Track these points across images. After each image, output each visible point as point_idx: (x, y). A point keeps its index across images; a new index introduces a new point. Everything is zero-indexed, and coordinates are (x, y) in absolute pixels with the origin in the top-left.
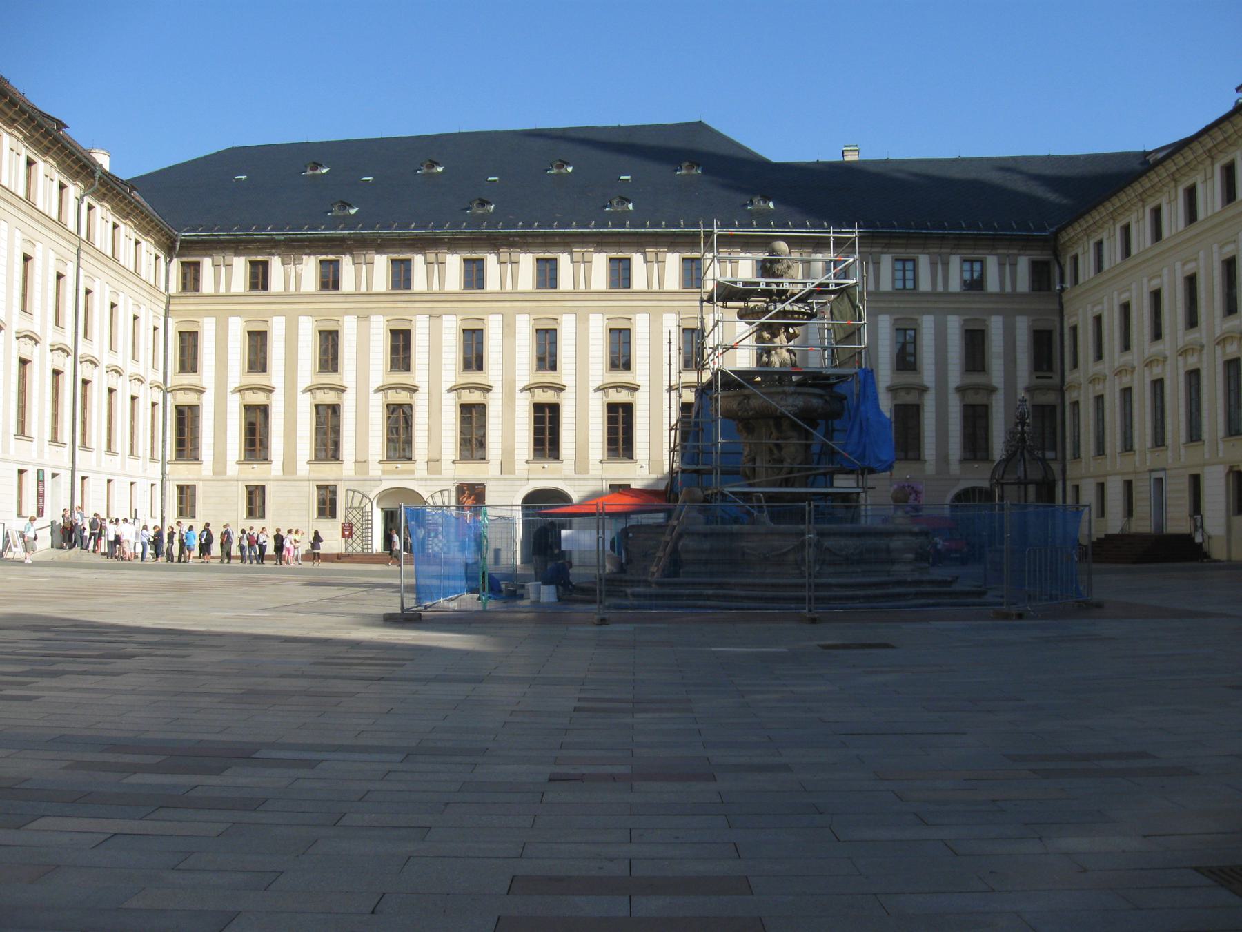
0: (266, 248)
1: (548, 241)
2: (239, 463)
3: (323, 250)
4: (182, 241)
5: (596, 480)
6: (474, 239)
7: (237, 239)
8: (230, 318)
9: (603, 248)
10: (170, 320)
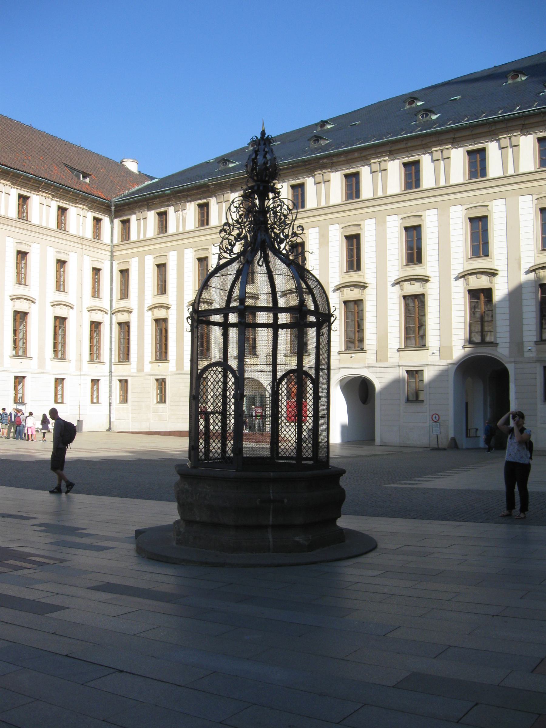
0: (163, 202)
1: (349, 157)
2: (151, 362)
3: (199, 197)
4: (116, 206)
5: (394, 367)
6: (293, 167)
7: (145, 198)
8: (146, 257)
9: (395, 155)
10: (115, 263)
